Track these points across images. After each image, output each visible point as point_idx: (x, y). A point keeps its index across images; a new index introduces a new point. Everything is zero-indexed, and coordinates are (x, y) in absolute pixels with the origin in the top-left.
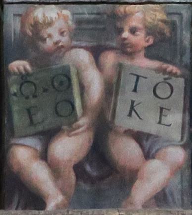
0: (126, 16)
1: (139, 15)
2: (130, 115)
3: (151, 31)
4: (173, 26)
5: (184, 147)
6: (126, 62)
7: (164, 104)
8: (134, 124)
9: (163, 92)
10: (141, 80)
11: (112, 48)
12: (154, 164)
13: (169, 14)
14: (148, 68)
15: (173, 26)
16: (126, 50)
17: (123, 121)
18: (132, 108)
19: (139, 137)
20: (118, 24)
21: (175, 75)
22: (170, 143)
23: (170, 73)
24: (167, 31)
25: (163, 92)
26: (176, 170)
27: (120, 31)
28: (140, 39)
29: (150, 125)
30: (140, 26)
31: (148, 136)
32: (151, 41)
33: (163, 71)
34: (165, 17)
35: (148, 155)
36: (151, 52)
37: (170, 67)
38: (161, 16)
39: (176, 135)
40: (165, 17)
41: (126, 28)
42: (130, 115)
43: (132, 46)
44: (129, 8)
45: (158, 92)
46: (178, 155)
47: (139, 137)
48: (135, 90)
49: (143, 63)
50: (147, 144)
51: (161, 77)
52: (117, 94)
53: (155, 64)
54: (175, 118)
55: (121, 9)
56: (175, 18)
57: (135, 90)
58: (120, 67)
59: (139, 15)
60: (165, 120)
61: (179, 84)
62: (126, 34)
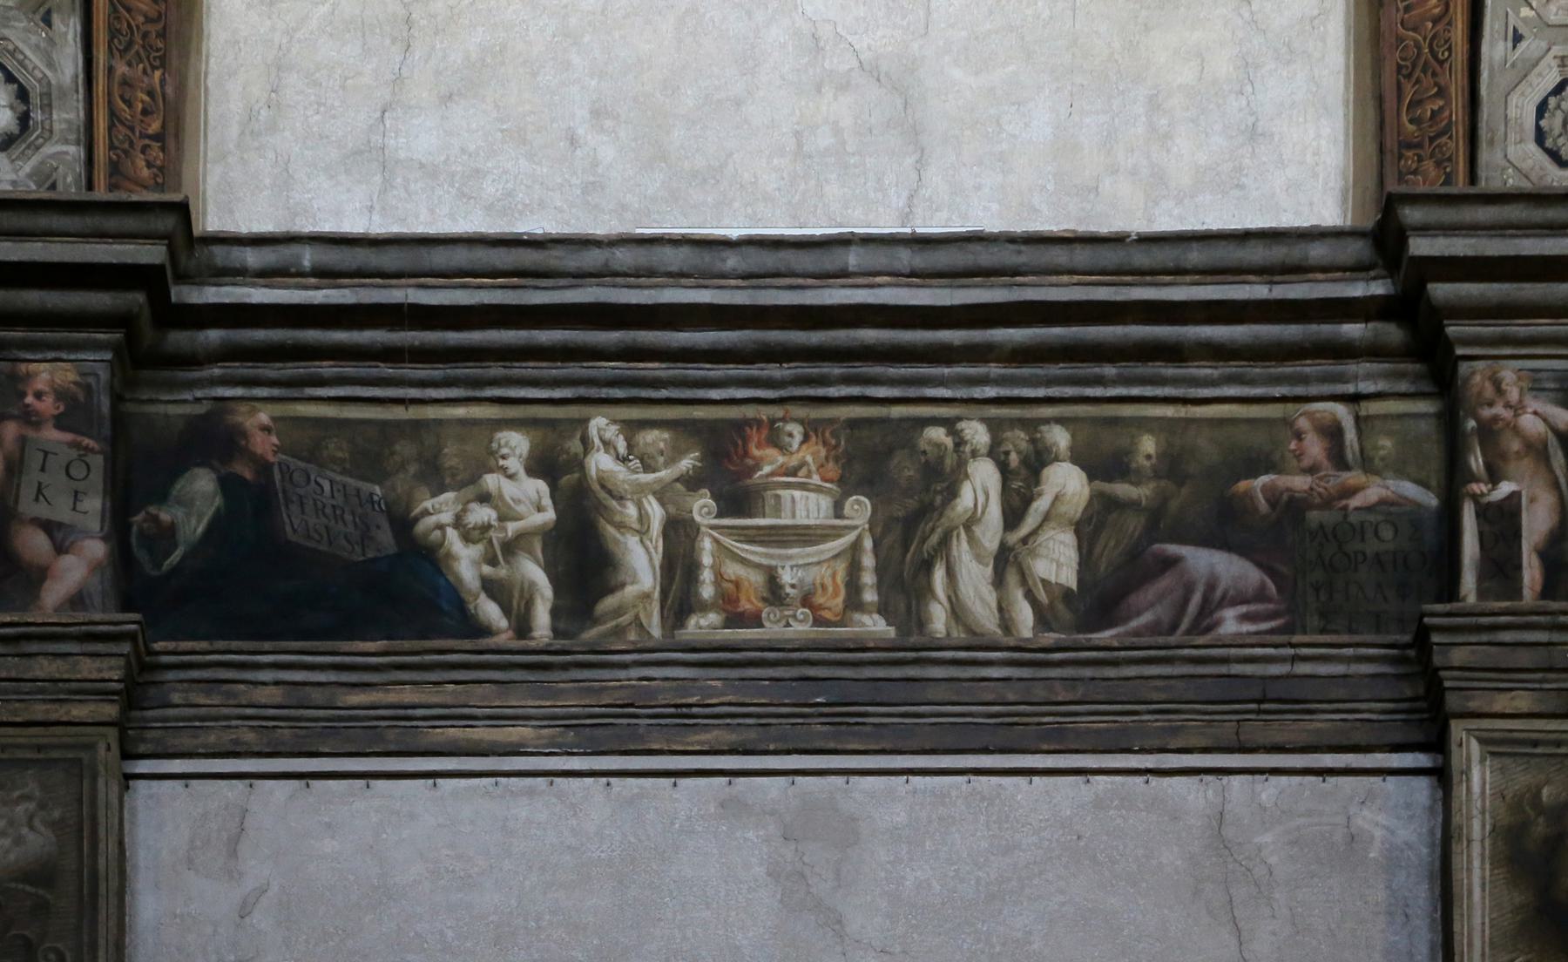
0: (29, 376)
1: (45, 376)
2: (37, 499)
3: (61, 394)
4: (88, 389)
5: (104, 539)
6: (31, 433)
7: (81, 486)
8: (42, 510)
9: (78, 471)
10: (50, 456)
11: (11, 417)
12: (68, 560)
13: (83, 375)
14: (59, 442)
15: (88, 389)
16: (29, 418)
17: (28, 506)
18: (39, 491)
19: (48, 527)
20: (20, 387)
21: (92, 451)
22: (89, 535)
23: (87, 448)
24: (81, 397)
25: (78, 471)
26: (96, 568)
27: (23, 395)
28: (48, 406)
29: (61, 511)
30: (47, 389)
31: (60, 525)
32: (62, 409)
33: (75, 445)
34: (78, 379)
35: (60, 549)
36: (61, 423)
37: (86, 441)
38: (72, 376)
39: (95, 525)
40: (78, 379)
41: (30, 392)
42: (37, 499)
43: (37, 413)
44: (33, 367)
45: (73, 472)
46: (96, 549)
47: (48, 527)
48: (43, 469)
49: (51, 434)
50: (59, 536)
51: (74, 453)
52: (21, 472)
53: (69, 437)
54: (94, 504)
55: (23, 367)
56: (91, 380)
57: (43, 469)
58: (23, 441)
59: (45, 376)
60: (80, 506)
61: (97, 461)
62: (29, 399)
